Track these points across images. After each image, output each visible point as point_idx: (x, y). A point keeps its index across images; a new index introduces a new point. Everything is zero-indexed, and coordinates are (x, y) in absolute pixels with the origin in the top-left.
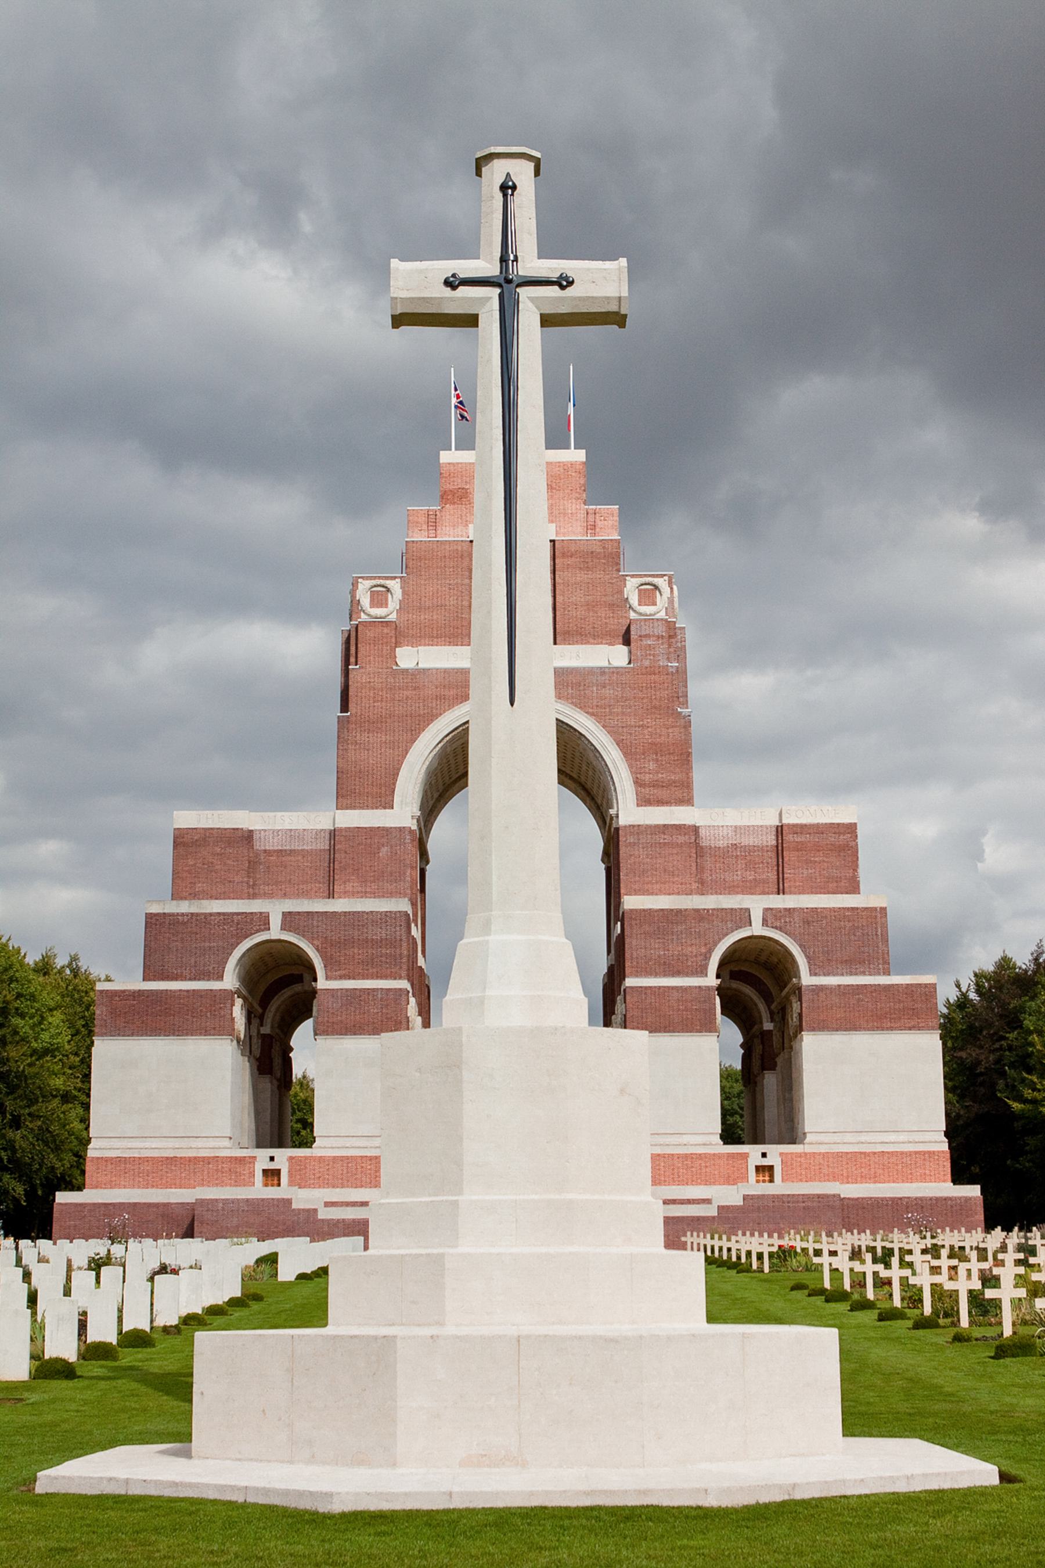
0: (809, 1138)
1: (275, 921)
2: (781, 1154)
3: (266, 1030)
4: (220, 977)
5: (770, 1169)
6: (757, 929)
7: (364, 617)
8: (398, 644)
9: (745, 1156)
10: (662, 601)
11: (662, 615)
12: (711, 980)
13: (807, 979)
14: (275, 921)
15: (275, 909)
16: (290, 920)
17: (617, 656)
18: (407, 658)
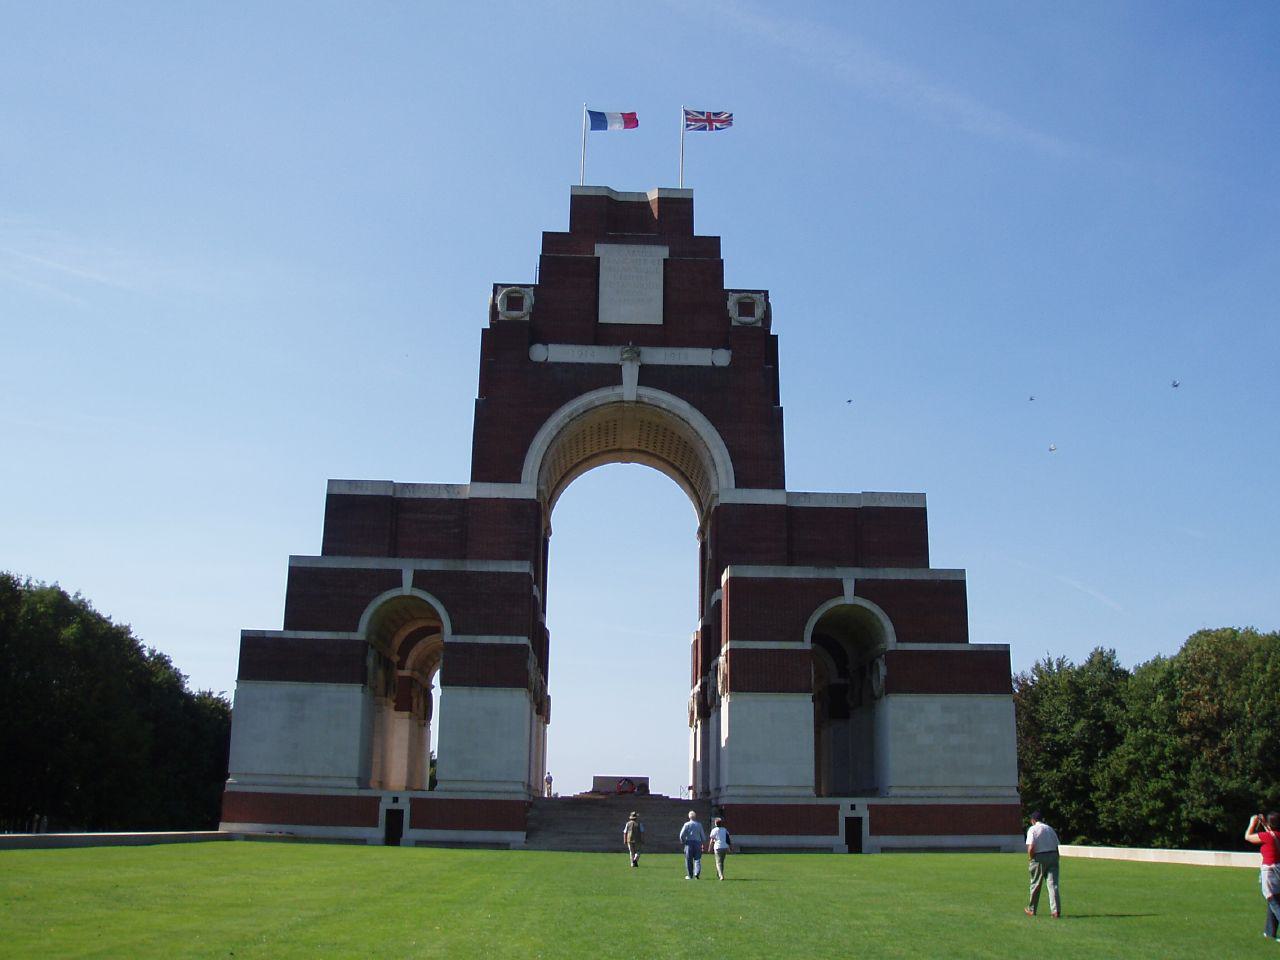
0: (894, 791)
1: (408, 578)
2: (870, 807)
3: (405, 673)
4: (355, 629)
5: (859, 820)
6: (849, 597)
7: (501, 318)
8: (532, 343)
9: (837, 807)
10: (759, 312)
11: (760, 324)
12: (806, 645)
13: (891, 642)
14: (408, 578)
15: (408, 568)
16: (420, 580)
17: (722, 358)
18: (539, 353)
